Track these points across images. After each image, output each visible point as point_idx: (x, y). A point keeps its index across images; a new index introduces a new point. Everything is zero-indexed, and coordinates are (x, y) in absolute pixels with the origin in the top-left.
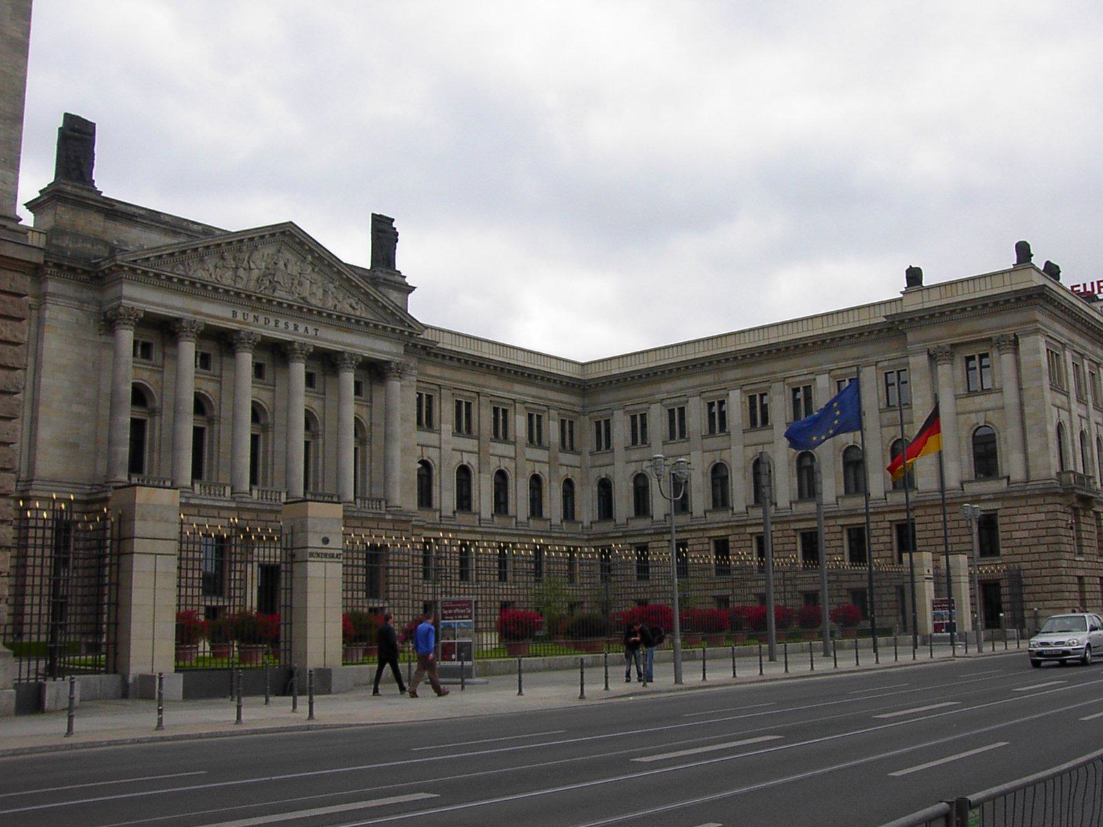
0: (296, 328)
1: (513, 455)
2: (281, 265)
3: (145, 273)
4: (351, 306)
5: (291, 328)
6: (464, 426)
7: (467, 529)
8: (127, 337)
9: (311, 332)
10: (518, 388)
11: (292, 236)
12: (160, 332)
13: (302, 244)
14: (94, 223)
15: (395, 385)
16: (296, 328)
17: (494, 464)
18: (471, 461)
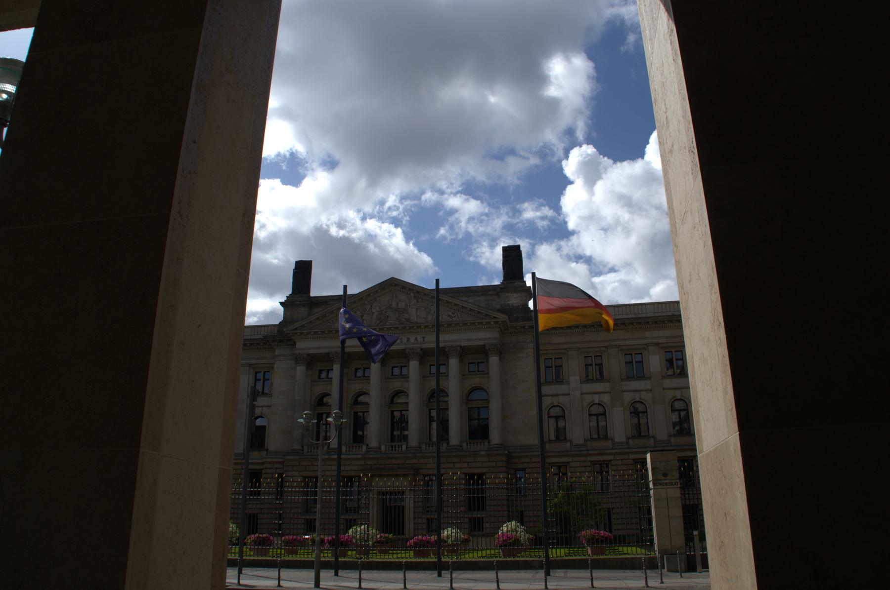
0: (408, 340)
1: (649, 387)
2: (394, 304)
3: (302, 333)
4: (449, 316)
5: (405, 340)
6: (595, 372)
7: (596, 452)
8: (301, 370)
9: (420, 339)
10: (648, 334)
11: (396, 285)
12: (316, 363)
13: (403, 287)
14: (304, 311)
15: (494, 360)
16: (408, 340)
17: (628, 397)
18: (606, 399)
